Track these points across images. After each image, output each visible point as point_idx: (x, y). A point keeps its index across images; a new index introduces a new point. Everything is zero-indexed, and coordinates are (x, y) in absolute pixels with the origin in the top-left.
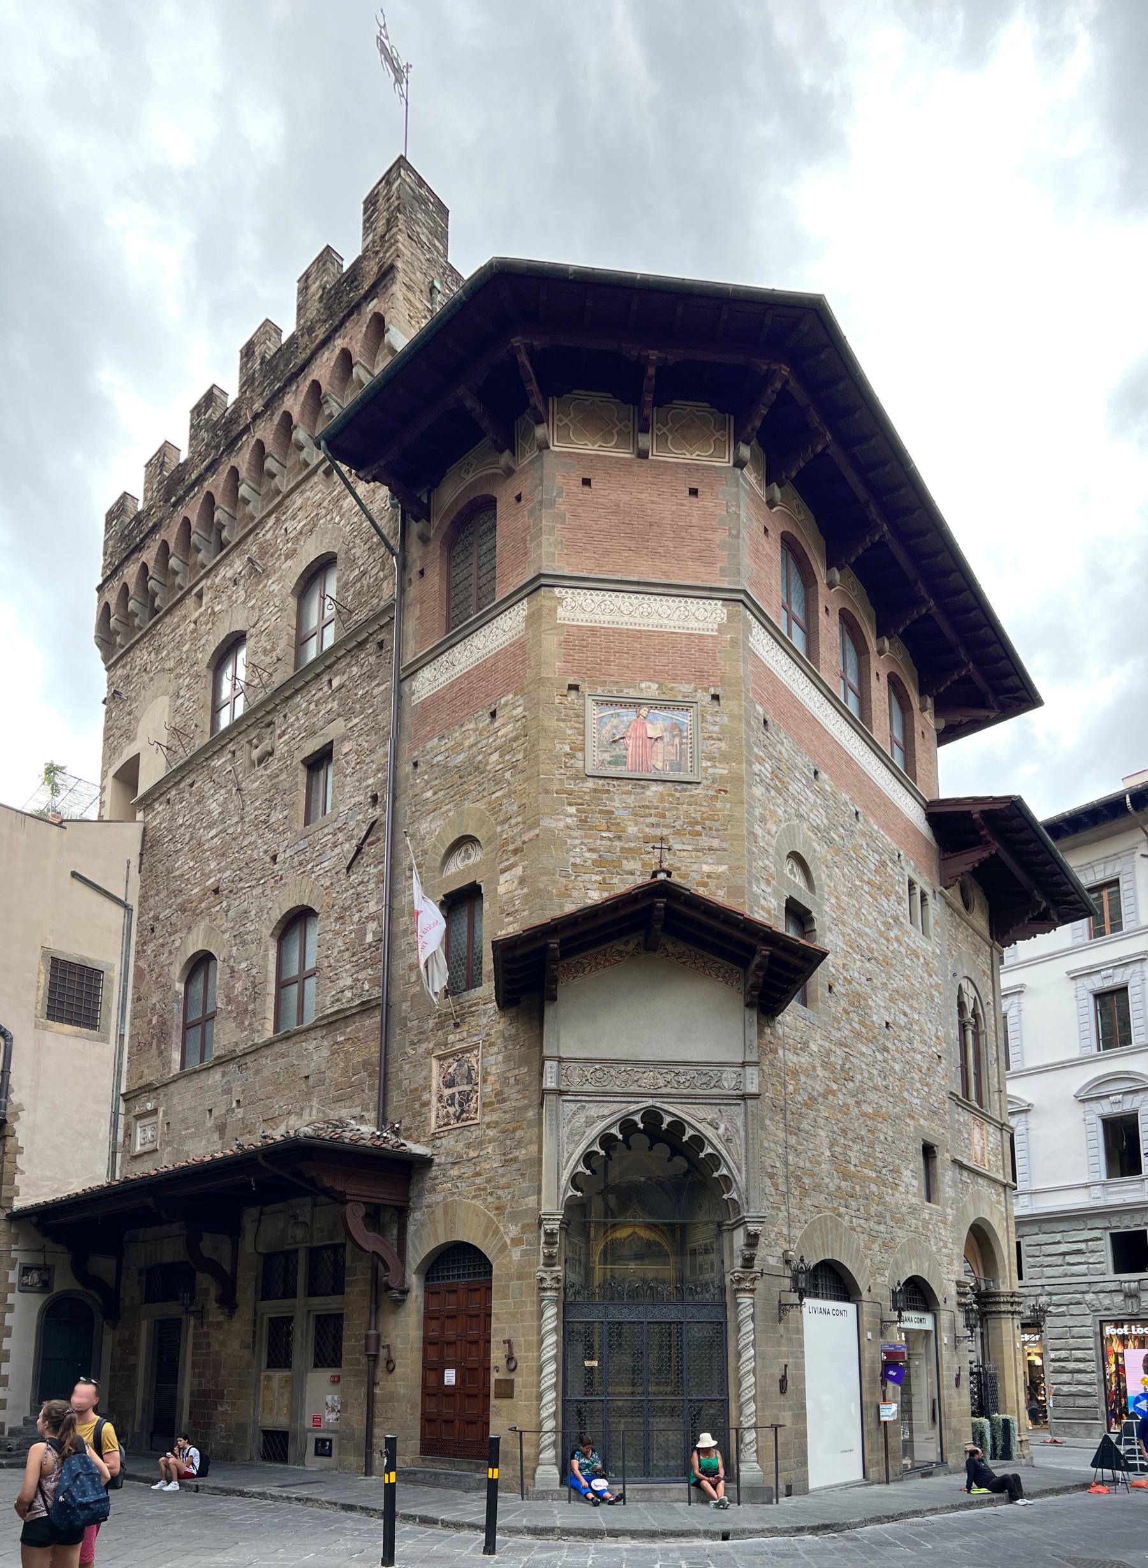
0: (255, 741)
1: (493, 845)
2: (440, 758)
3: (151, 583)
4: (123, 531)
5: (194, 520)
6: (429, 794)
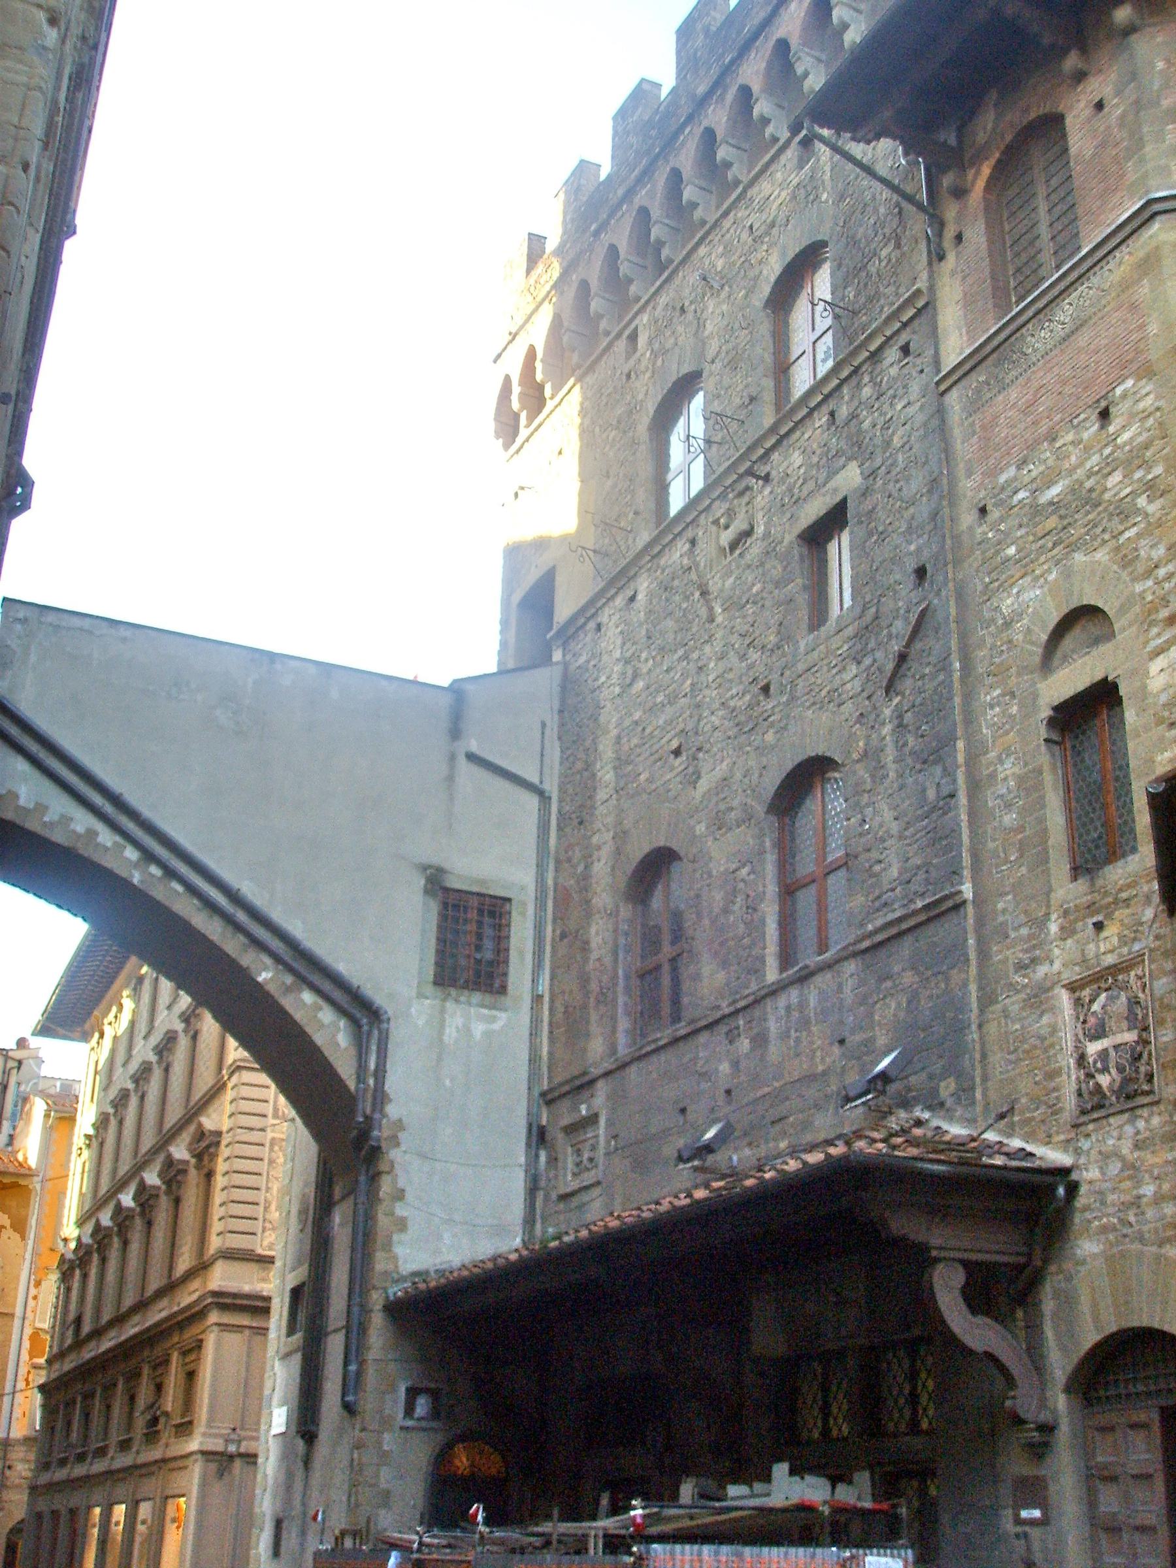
1: (1130, 616)
2: (1021, 495)
6: (1012, 551)
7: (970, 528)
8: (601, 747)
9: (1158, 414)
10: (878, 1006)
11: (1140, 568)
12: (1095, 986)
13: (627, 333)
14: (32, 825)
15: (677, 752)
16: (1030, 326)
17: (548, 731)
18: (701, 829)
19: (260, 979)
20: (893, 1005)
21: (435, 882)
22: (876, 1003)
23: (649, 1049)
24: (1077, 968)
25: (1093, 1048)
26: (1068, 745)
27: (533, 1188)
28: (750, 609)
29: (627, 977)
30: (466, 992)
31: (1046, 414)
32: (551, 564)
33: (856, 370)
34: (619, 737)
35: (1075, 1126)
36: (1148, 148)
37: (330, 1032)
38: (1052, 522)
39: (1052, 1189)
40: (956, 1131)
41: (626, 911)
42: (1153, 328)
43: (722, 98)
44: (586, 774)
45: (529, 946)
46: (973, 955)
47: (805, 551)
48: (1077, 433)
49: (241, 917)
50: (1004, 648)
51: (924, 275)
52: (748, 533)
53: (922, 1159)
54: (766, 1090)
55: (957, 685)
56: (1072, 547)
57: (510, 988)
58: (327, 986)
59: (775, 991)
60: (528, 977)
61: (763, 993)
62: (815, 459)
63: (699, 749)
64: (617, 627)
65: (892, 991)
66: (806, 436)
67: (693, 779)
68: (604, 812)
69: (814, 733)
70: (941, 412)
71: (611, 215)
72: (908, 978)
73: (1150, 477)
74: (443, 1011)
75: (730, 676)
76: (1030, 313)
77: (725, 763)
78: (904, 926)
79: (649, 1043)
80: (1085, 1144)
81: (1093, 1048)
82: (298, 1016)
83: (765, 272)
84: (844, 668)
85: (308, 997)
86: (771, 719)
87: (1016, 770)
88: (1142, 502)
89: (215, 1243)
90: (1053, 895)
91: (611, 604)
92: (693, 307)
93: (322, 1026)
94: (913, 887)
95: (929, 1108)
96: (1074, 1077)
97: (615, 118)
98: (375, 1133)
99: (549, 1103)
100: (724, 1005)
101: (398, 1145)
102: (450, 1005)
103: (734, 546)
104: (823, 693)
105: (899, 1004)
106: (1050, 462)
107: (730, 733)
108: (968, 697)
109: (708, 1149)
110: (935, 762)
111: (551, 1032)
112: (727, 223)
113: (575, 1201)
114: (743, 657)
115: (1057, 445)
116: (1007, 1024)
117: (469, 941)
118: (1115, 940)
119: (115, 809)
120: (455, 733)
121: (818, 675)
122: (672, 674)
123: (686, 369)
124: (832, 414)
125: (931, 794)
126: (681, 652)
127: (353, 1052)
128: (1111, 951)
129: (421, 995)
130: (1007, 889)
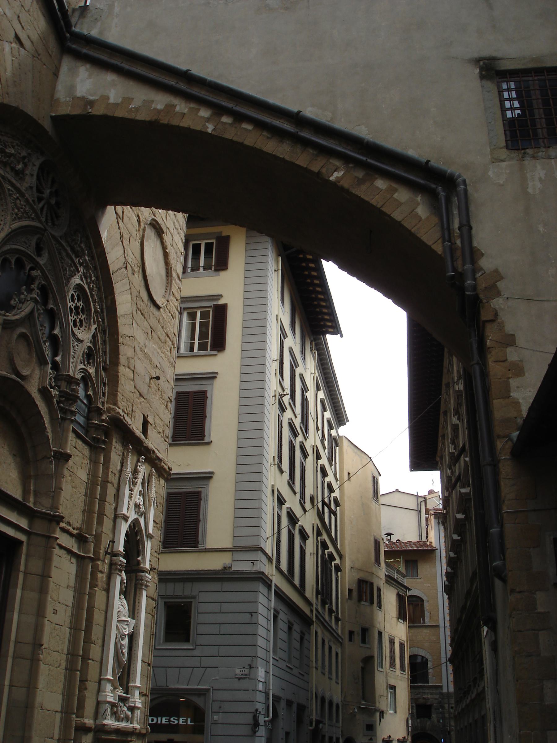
14: (120, 113)
19: (331, 179)
21: (490, 70)
37: (409, 209)
85: (381, 184)
93: (400, 204)
102: (528, 162)
127: (435, 220)
129: (496, 160)
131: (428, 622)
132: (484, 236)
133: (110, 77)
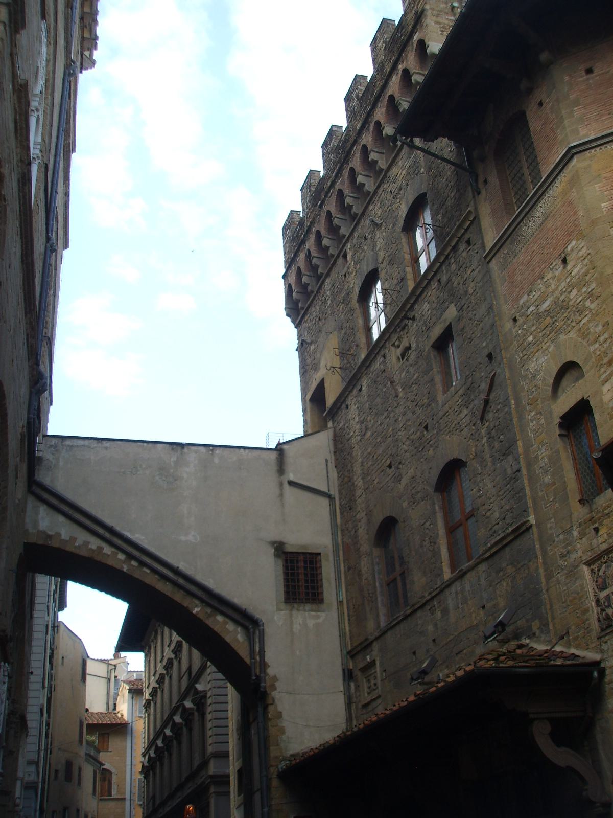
0: (397, 343)
2: (532, 309)
3: (314, 261)
4: (293, 235)
5: (333, 210)
6: (531, 339)
7: (510, 330)
8: (355, 469)
9: (589, 257)
10: (498, 586)
11: (592, 338)
12: (599, 562)
13: (342, 254)
14: (69, 548)
15: (390, 466)
16: (524, 221)
17: (329, 464)
18: (405, 504)
19: (194, 612)
20: (505, 584)
21: (279, 549)
22: (497, 584)
23: (394, 623)
24: (589, 554)
25: (603, 595)
26: (572, 436)
27: (349, 703)
28: (415, 387)
29: (381, 586)
30: (302, 605)
31: (538, 264)
32: (322, 378)
33: (447, 256)
34: (362, 462)
35: (599, 638)
36: (566, 122)
37: (234, 635)
38: (548, 320)
39: (592, 673)
40: (541, 647)
41: (377, 552)
42: (581, 213)
43: (368, 129)
44: (350, 484)
45: (332, 575)
46: (539, 553)
47: (436, 353)
48: (553, 273)
49: (181, 581)
50: (534, 389)
51: (472, 203)
52: (409, 348)
53: (516, 667)
54: (451, 637)
55: (514, 412)
56: (558, 332)
57: (326, 600)
58: (230, 612)
59: (449, 585)
60: (334, 592)
61: (443, 587)
62: (434, 305)
63: (400, 463)
64: (355, 406)
65: (504, 577)
66: (429, 294)
67: (398, 479)
68: (360, 503)
69: (451, 446)
70: (488, 272)
71: (326, 196)
72: (510, 570)
73: (590, 290)
74: (291, 616)
75: (409, 423)
76: (523, 215)
77: (412, 469)
78: (505, 542)
79: (394, 619)
80: (605, 647)
81: (603, 595)
82: (216, 628)
83: (400, 213)
84: (461, 411)
85: (220, 618)
86: (431, 443)
87: (547, 453)
88: (588, 303)
89: (210, 749)
90: (572, 516)
91: (351, 394)
92: (370, 236)
94: (508, 521)
95: (529, 637)
96: (595, 611)
97: (322, 147)
98: (263, 684)
99: (352, 657)
100: (426, 595)
101: (275, 689)
102: (294, 613)
103: (403, 355)
104: (453, 426)
105: (508, 584)
106: (543, 290)
107: (413, 453)
108: (521, 418)
109: (424, 672)
110: (508, 455)
111: (349, 620)
112: (380, 191)
113: (370, 708)
114: (414, 412)
115: (545, 280)
116: (560, 587)
117: (300, 577)
118: (605, 536)
119: (111, 535)
120: (281, 470)
121: (449, 417)
122: (383, 426)
123: (370, 268)
124: (439, 281)
125: (509, 471)
126: (385, 414)
127: (246, 644)
128: (605, 542)
129: (279, 609)
130: (551, 516)
131: (114, 794)
132: (269, 657)
133: (61, 519)
